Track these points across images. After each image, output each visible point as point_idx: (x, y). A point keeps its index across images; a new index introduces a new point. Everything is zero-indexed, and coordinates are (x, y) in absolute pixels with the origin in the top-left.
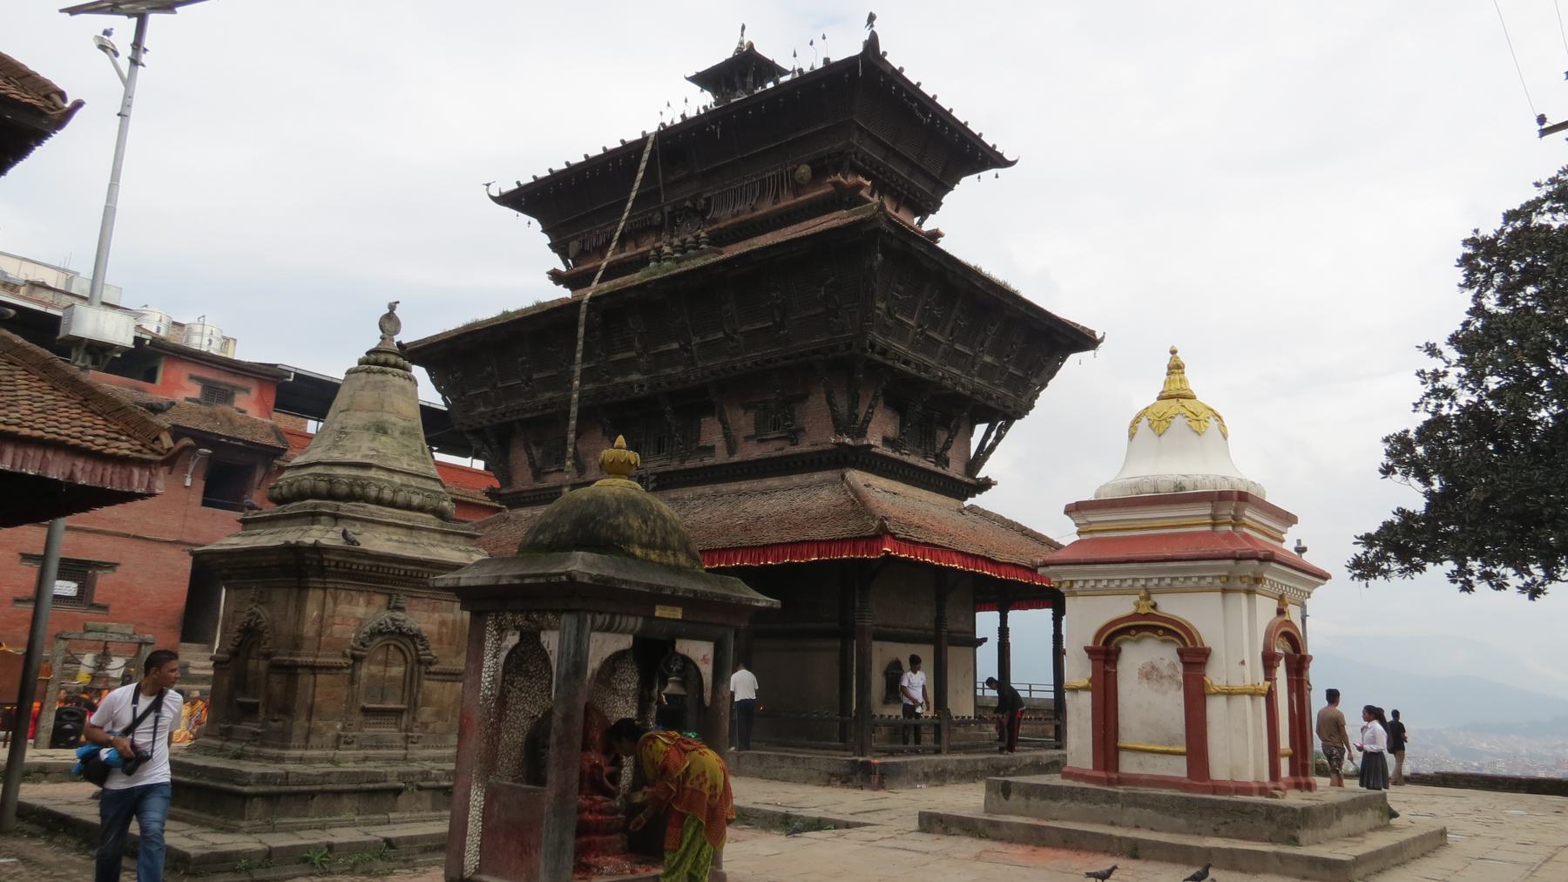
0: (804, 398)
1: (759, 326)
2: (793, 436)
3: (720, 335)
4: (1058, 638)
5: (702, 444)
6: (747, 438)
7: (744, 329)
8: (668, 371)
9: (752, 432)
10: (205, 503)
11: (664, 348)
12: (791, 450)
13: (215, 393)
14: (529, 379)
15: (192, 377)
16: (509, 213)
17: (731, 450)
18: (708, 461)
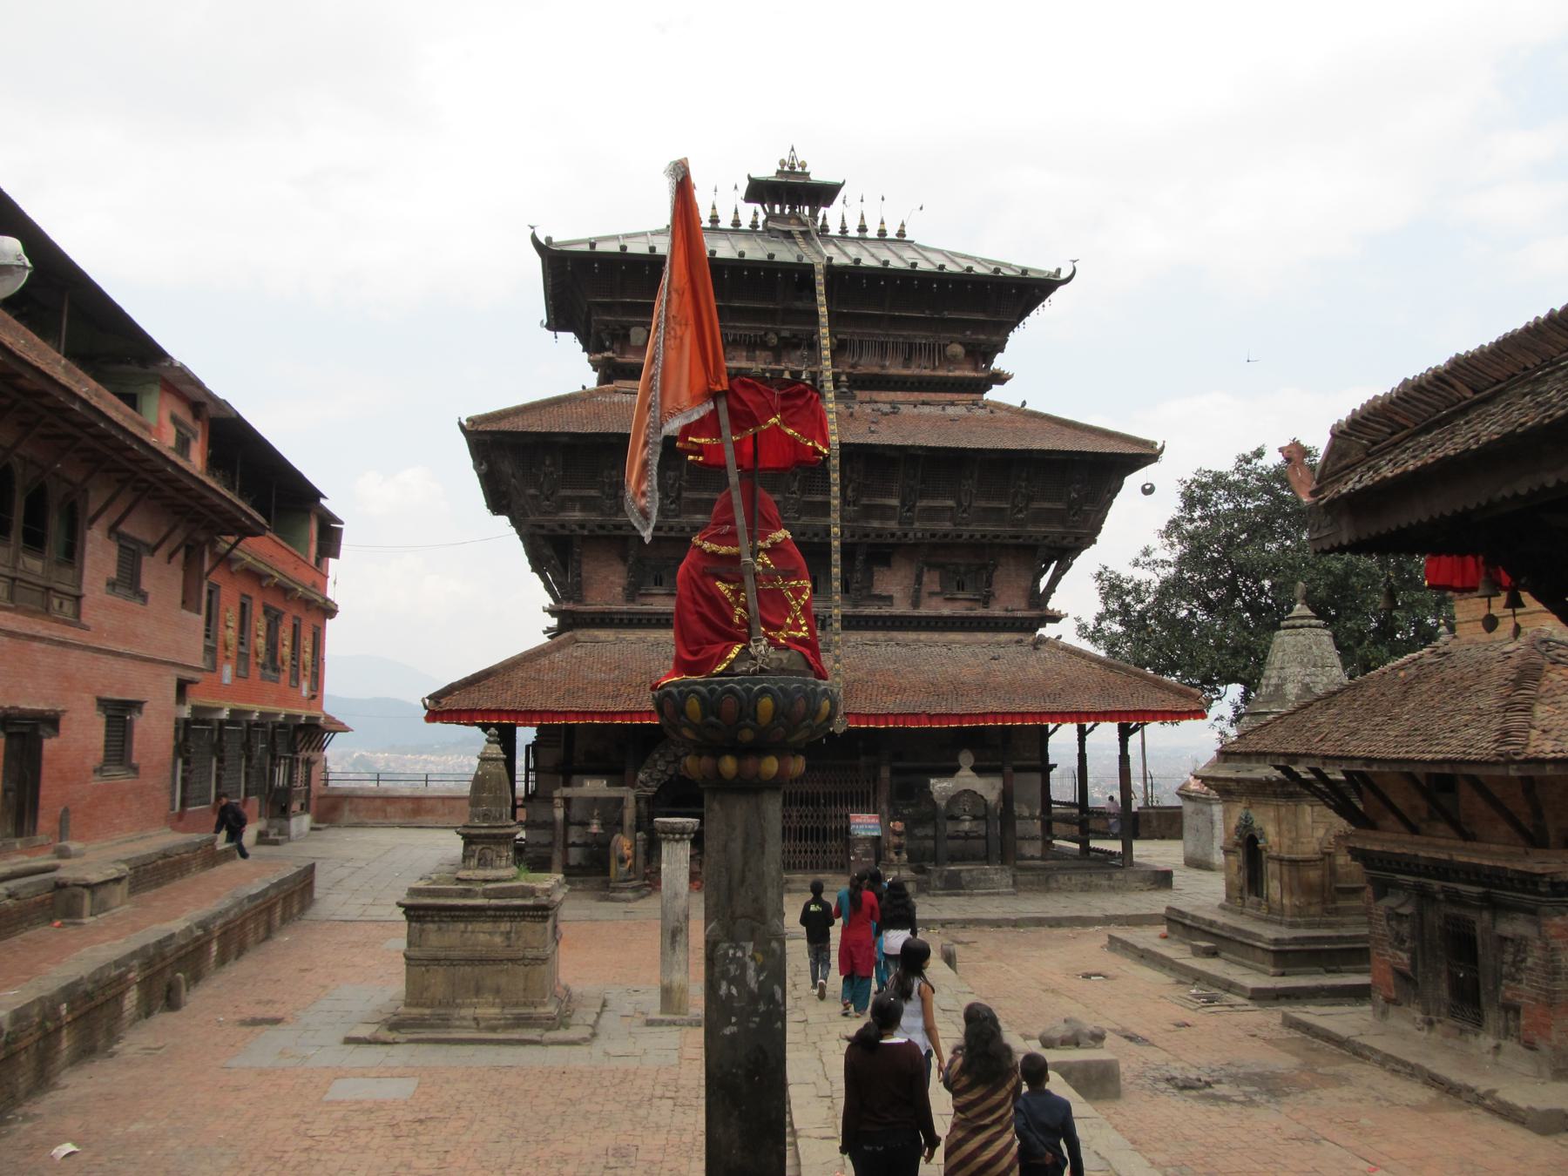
0: (996, 567)
1: (995, 504)
2: (986, 604)
3: (950, 503)
4: (1124, 758)
5: (877, 592)
6: (932, 594)
7: (984, 504)
8: (876, 524)
9: (937, 588)
10: (185, 604)
11: (879, 501)
12: (980, 612)
13: (183, 445)
14: (678, 497)
15: (175, 420)
16: (537, 261)
17: (916, 605)
18: (885, 611)
